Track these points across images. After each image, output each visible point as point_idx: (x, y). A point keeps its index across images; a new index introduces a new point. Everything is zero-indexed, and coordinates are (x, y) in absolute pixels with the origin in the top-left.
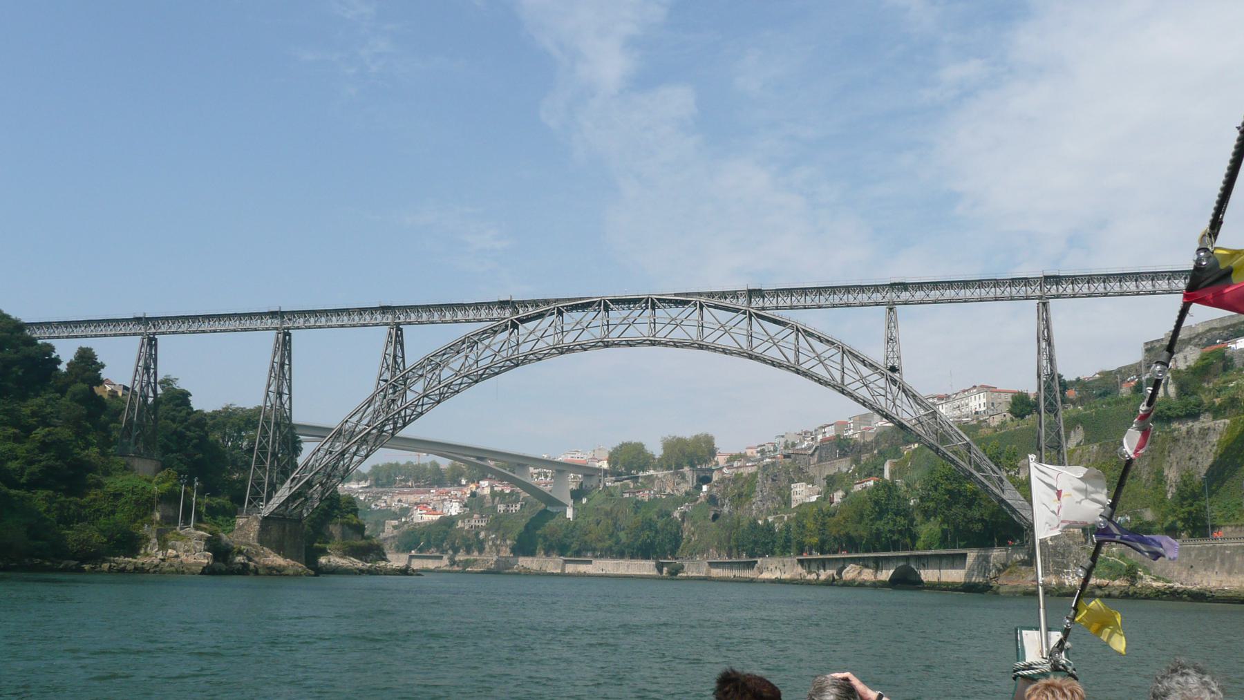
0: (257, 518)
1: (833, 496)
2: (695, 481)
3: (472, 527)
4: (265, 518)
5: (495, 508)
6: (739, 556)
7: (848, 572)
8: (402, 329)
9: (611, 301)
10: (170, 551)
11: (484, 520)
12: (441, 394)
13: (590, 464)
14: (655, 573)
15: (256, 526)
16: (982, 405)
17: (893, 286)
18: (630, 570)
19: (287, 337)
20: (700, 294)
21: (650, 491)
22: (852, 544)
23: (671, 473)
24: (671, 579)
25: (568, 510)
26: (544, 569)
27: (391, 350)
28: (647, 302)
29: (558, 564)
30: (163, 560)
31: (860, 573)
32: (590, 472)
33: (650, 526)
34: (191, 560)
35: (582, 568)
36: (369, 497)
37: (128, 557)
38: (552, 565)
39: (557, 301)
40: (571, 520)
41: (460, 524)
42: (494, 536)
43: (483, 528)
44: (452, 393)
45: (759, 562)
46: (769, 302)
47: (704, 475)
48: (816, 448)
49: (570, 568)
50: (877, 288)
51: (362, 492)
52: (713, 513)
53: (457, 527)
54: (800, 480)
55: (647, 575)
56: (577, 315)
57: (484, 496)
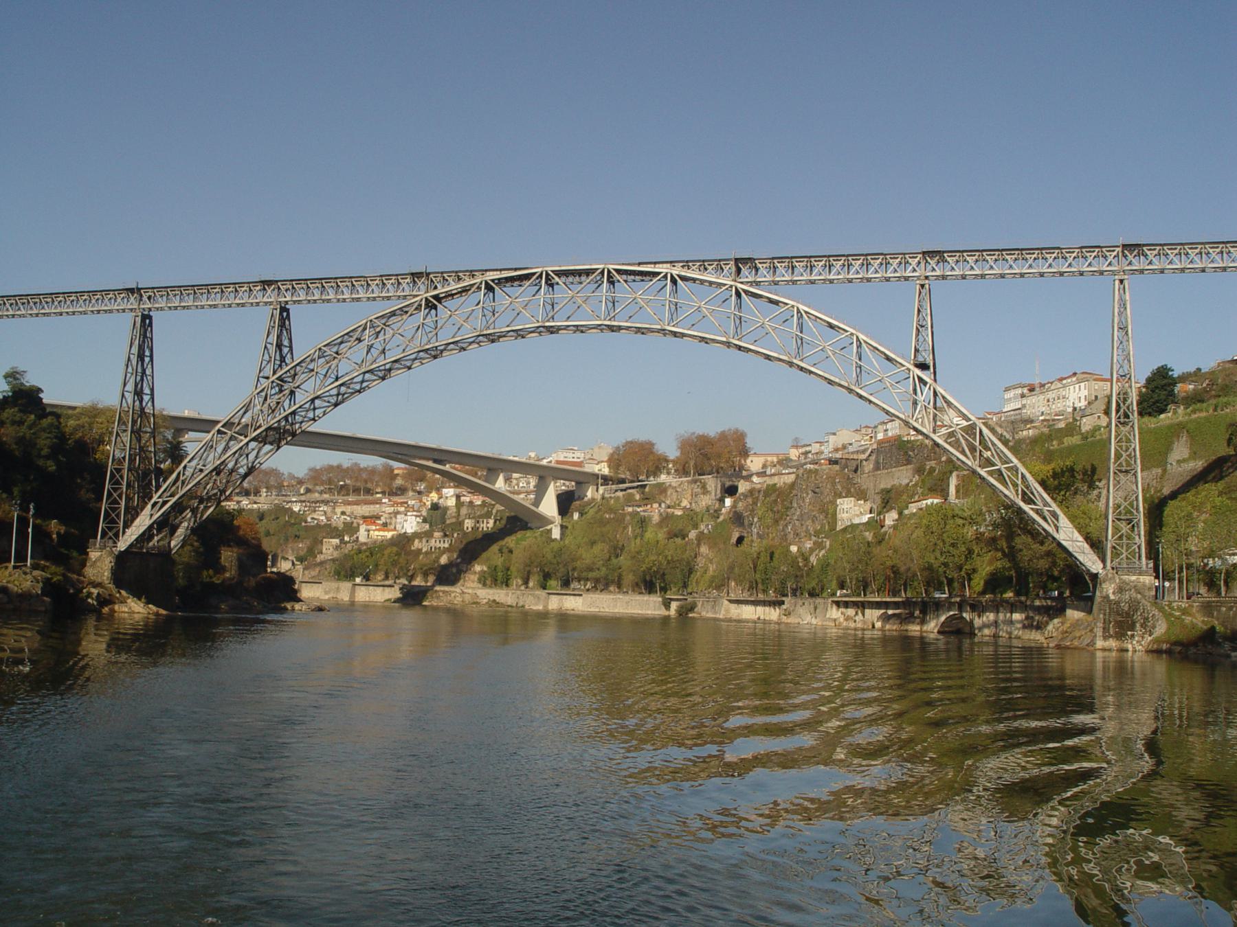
1: (884, 517)
2: (719, 492)
5: (461, 524)
6: (765, 591)
8: (289, 309)
11: (446, 540)
12: (338, 395)
16: (1083, 399)
19: (147, 321)
21: (660, 505)
23: (688, 482)
27: (273, 338)
32: (585, 480)
36: (306, 506)
41: (417, 544)
44: (353, 393)
47: (731, 483)
51: (296, 502)
52: (736, 536)
53: (413, 548)
57: (446, 509)
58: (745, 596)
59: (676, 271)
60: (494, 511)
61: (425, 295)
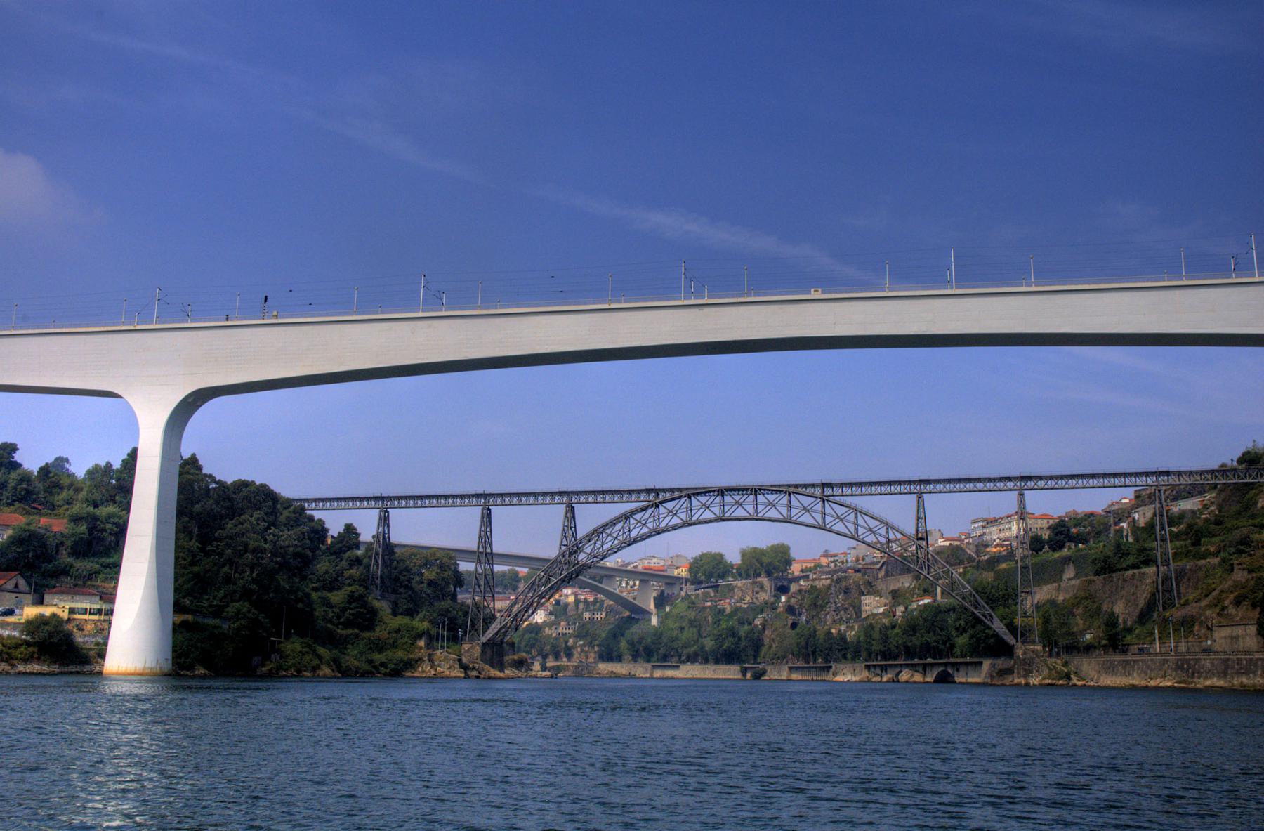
4: (484, 644)
5: (580, 616)
6: (815, 661)
10: (438, 669)
13: (669, 573)
14: (740, 676)
15: (478, 650)
17: (921, 482)
20: (789, 486)
22: (909, 652)
28: (751, 490)
29: (646, 669)
31: (912, 676)
32: (672, 581)
33: (733, 633)
35: (669, 673)
38: (641, 670)
39: (687, 489)
42: (581, 643)
45: (834, 667)
46: (837, 491)
48: (883, 564)
49: (658, 673)
50: (910, 483)
52: (790, 622)
54: (869, 593)
56: (703, 499)
57: (567, 605)
59: (791, 489)
60: (605, 606)
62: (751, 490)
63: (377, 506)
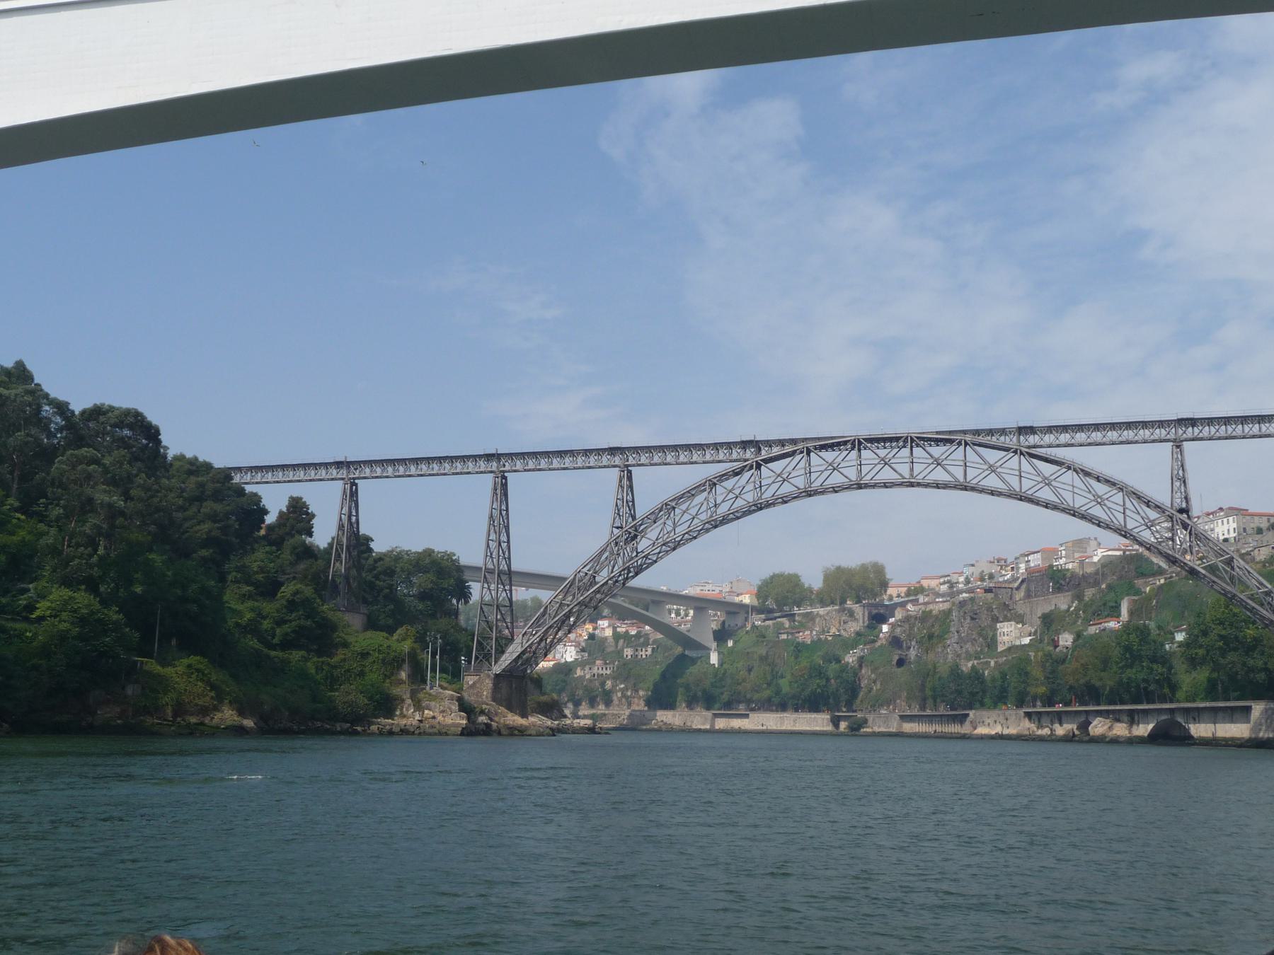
0: (489, 676)
1: (1058, 638)
2: (866, 619)
3: (594, 675)
4: (497, 675)
5: (619, 653)
6: (936, 707)
7: (1096, 727)
8: (631, 471)
9: (866, 440)
10: (426, 712)
13: (729, 599)
14: (830, 728)
15: (488, 684)
16: (1232, 531)
17: (1182, 422)
18: (797, 725)
20: (965, 432)
21: (811, 632)
22: (1090, 694)
23: (835, 610)
24: (853, 735)
25: (711, 654)
26: (689, 724)
29: (706, 719)
30: (421, 721)
31: (1110, 728)
32: (734, 610)
33: (820, 673)
34: (449, 721)
35: (736, 723)
37: (388, 719)
38: (699, 719)
40: (716, 666)
41: (579, 672)
42: (622, 686)
43: (608, 677)
47: (877, 611)
48: (1023, 581)
49: (721, 724)
50: (1161, 424)
52: (896, 658)
53: (576, 676)
54: (1006, 619)
55: (820, 731)
56: (829, 455)
57: (606, 638)
58: (942, 710)
59: (969, 438)
61: (755, 460)
62: (905, 441)
63: (339, 476)
